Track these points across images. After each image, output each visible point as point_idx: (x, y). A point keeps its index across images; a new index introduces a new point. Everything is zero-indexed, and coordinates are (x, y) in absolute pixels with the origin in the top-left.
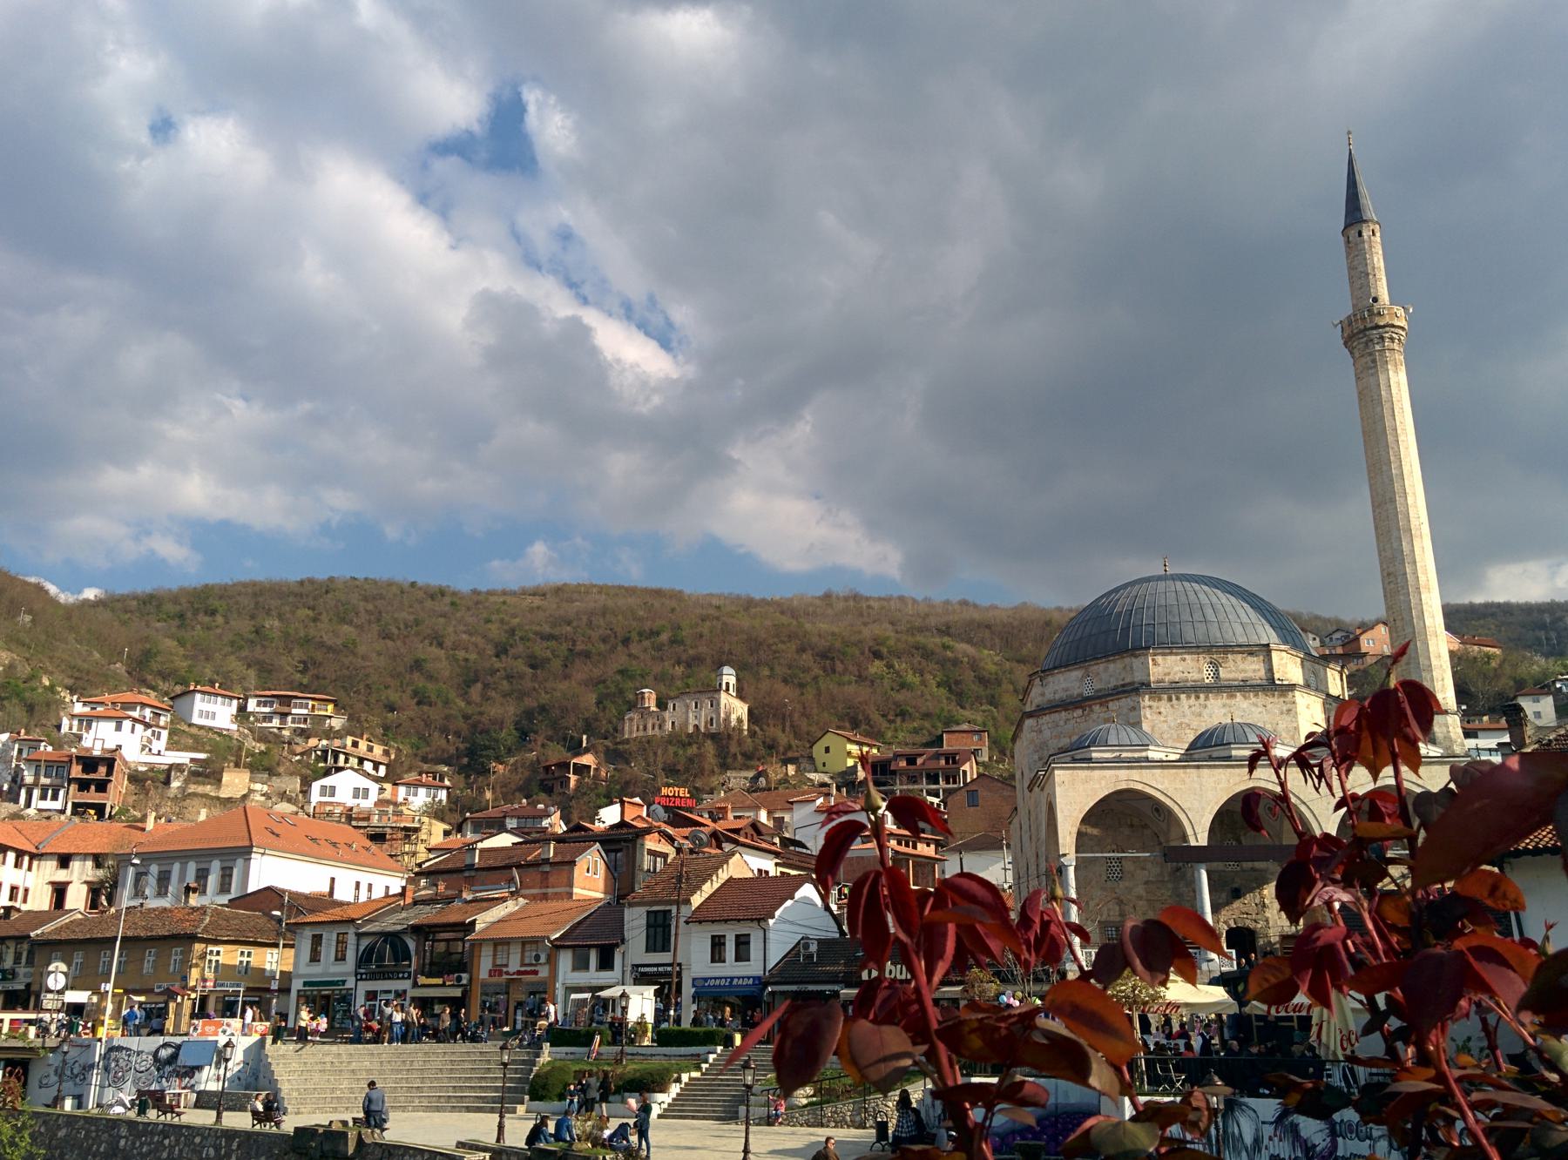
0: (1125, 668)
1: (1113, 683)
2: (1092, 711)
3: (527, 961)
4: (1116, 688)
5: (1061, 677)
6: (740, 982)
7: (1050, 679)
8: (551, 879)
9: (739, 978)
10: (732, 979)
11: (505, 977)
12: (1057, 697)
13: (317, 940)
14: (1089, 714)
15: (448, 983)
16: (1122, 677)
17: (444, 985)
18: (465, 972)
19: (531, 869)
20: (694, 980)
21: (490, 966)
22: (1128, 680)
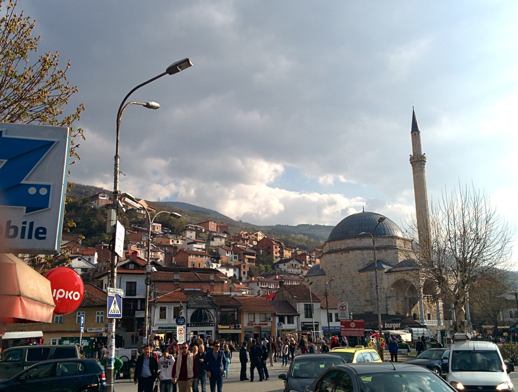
0: (389, 241)
1: (385, 245)
2: (382, 251)
3: (262, 320)
4: (386, 246)
5: (367, 240)
6: (338, 328)
7: (363, 239)
8: (215, 288)
9: (337, 327)
10: (335, 327)
11: (254, 326)
12: (365, 245)
13: (163, 310)
14: (380, 252)
15: (232, 328)
16: (388, 243)
17: (230, 328)
18: (241, 324)
19: (206, 284)
20: (323, 327)
21: (248, 322)
22: (390, 244)
